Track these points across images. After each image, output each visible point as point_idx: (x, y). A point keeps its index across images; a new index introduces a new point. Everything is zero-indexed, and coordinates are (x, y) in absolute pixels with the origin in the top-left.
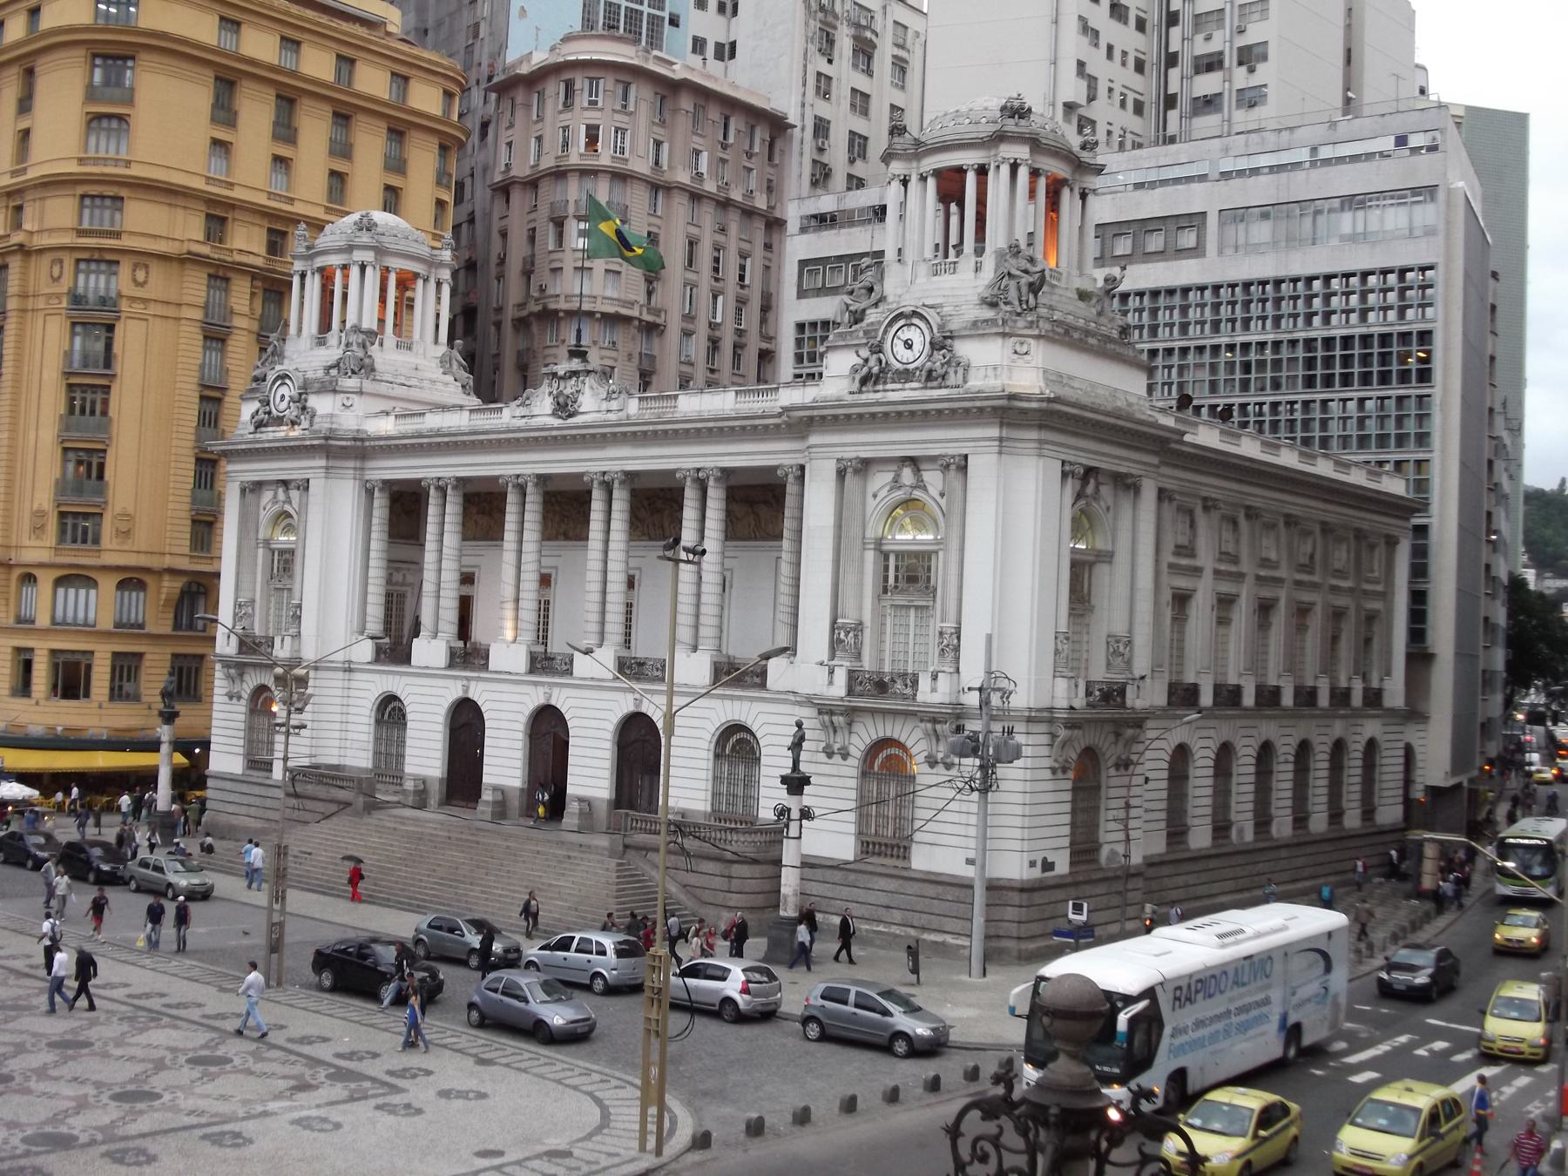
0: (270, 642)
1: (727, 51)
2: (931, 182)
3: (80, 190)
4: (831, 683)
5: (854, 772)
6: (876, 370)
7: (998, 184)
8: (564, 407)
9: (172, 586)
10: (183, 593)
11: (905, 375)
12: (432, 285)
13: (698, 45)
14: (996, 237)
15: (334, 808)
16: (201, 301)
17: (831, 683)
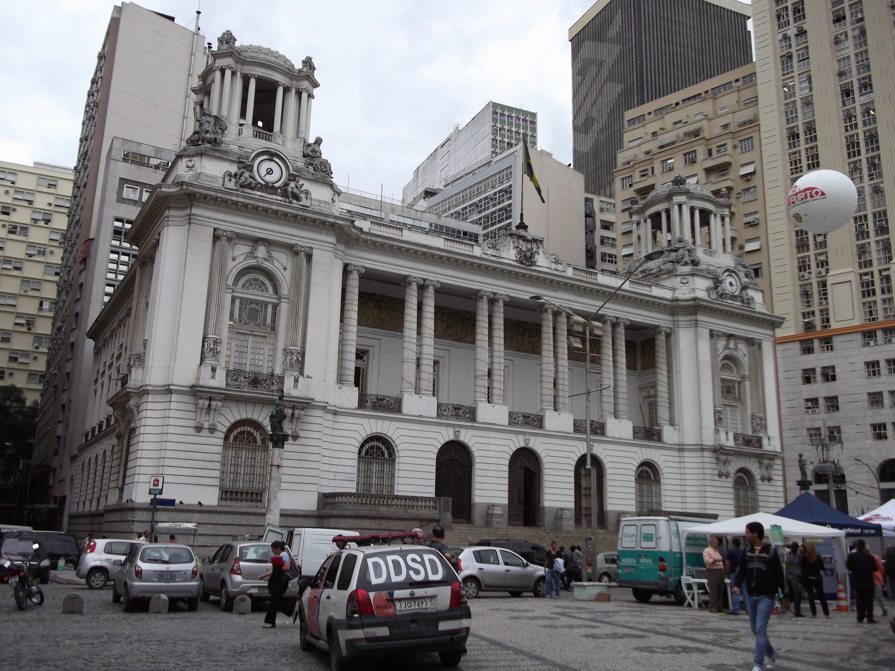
4: (213, 377)
11: (269, 188)
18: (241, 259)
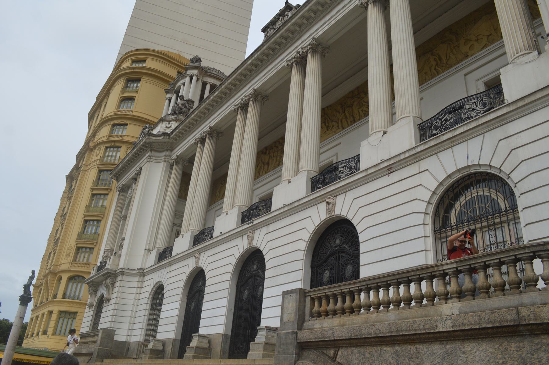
3: (112, 123)
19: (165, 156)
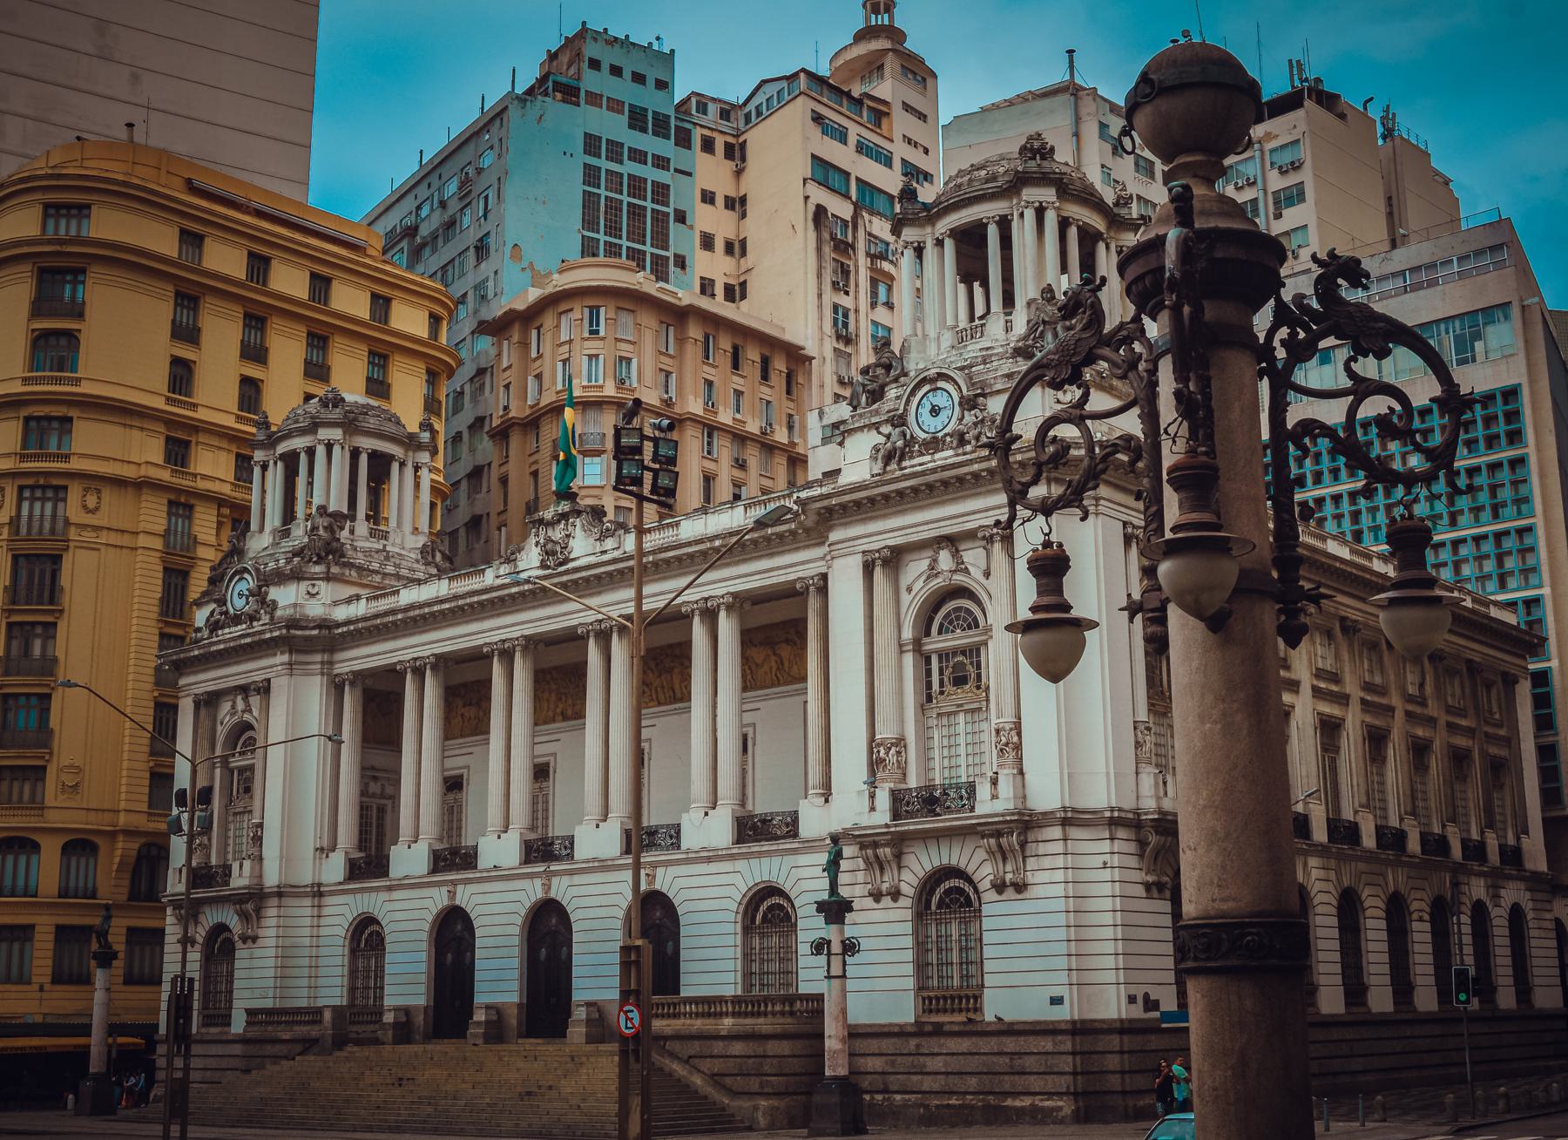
0: (227, 870)
1: (735, 292)
2: (949, 244)
3: (24, 412)
4: (873, 809)
5: (908, 914)
6: (900, 443)
7: (1023, 234)
8: (554, 555)
9: (124, 848)
10: (140, 857)
11: (934, 444)
12: (409, 470)
13: (707, 287)
14: (1026, 289)
15: (299, 1048)
16: (161, 529)
17: (873, 809)
18: (920, 583)
19: (322, 663)
